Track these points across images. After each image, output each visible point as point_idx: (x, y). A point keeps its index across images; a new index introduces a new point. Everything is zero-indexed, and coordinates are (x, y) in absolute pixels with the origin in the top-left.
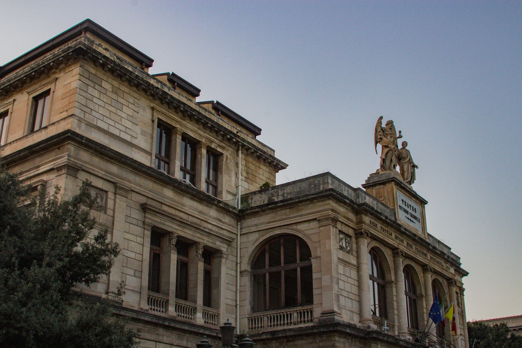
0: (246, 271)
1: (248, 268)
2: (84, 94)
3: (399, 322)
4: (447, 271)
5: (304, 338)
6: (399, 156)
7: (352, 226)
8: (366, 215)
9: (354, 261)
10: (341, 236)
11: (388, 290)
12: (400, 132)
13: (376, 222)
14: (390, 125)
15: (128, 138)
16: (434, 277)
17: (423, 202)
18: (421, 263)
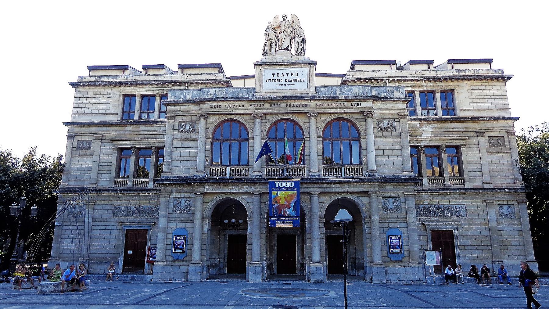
2: (78, 102)
8: (205, 104)
15: (104, 112)
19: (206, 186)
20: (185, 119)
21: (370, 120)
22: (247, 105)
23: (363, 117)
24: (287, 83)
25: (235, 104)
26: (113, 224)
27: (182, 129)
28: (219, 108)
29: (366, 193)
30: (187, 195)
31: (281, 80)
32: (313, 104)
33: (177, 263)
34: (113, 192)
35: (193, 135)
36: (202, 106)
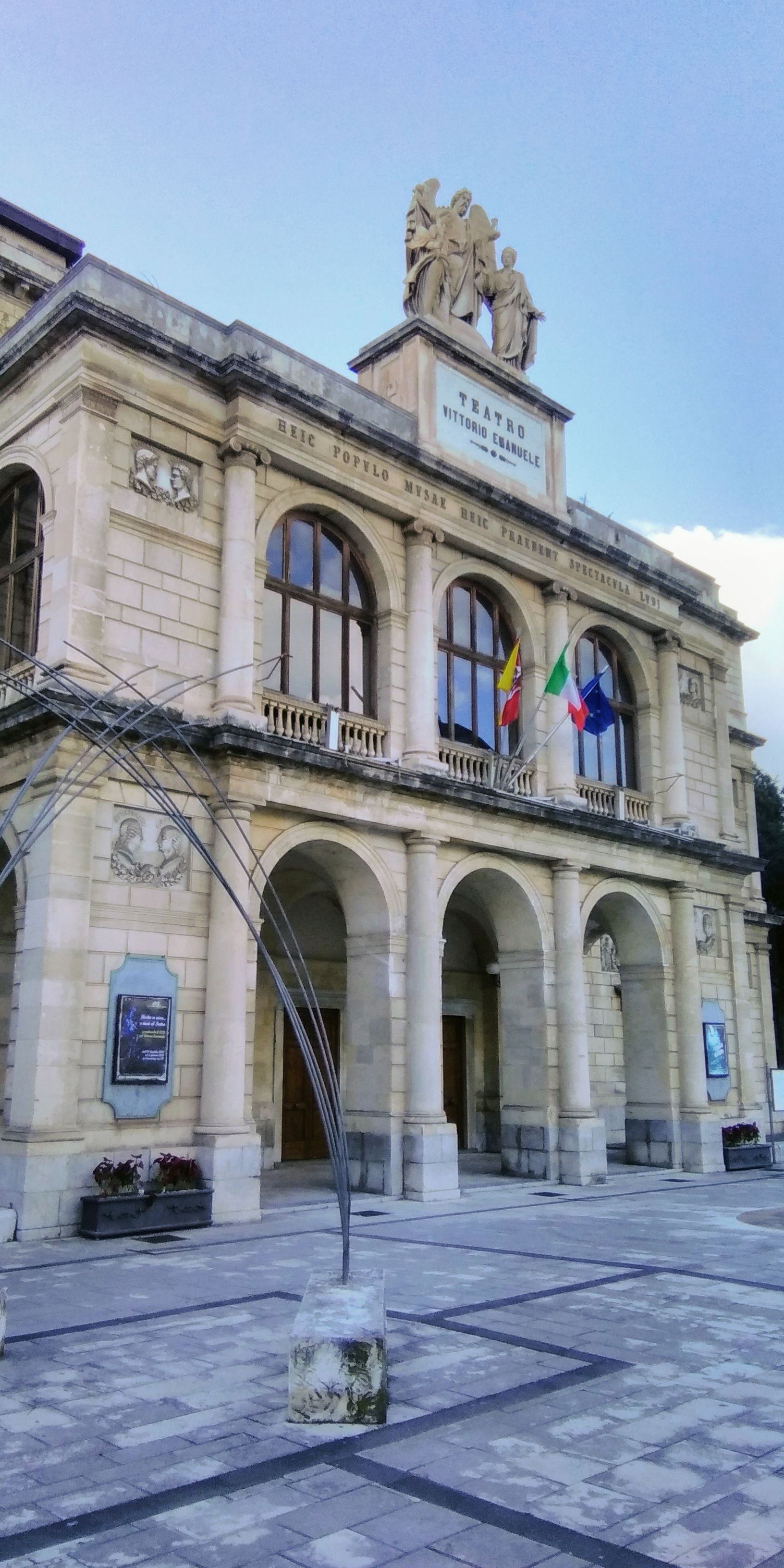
3: (407, 724)
4: (643, 607)
7: (202, 431)
9: (209, 537)
10: (146, 453)
13: (309, 430)
14: (461, 202)
16: (593, 619)
17: (556, 414)
18: (538, 579)
19: (274, 775)
20: (160, 433)
21: (672, 658)
22: (397, 477)
23: (653, 647)
24: (500, 451)
25: (361, 456)
27: (142, 476)
28: (306, 445)
29: (668, 886)
31: (483, 432)
32: (564, 557)
35: (196, 527)
36: (244, 405)
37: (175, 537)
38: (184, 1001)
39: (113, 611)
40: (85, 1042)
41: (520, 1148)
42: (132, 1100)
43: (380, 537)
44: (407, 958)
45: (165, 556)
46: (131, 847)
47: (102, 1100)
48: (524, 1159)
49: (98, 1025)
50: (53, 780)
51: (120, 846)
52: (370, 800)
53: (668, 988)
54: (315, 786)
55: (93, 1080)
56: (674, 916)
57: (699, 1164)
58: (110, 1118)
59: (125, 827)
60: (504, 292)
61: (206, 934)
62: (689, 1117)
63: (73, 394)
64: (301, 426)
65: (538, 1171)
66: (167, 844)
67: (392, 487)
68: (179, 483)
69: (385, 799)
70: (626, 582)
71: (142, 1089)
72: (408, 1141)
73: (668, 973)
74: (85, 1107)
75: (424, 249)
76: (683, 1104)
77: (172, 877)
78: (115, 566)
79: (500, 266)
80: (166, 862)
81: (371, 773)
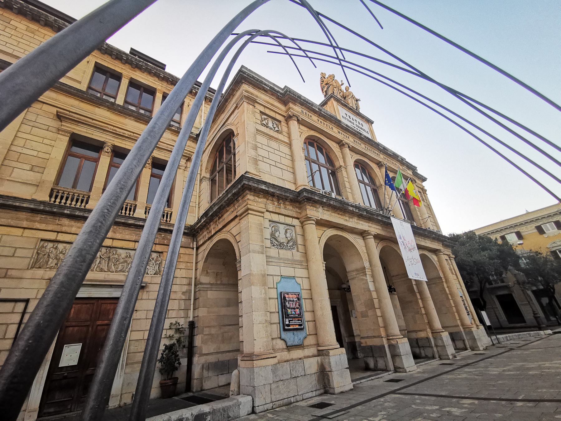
0: (204, 177)
1: (208, 176)
5: (228, 209)
6: (343, 95)
9: (286, 140)
11: (339, 175)
12: (342, 81)
13: (310, 114)
20: (267, 112)
22: (335, 130)
26: (25, 283)
27: (264, 122)
30: (289, 220)
33: (297, 354)
34: (36, 210)
37: (276, 139)
38: (304, 294)
39: (261, 158)
40: (270, 313)
41: (419, 347)
42: (292, 338)
43: (334, 146)
44: (373, 276)
45: (274, 144)
46: (277, 235)
47: (280, 338)
48: (422, 352)
49: (274, 305)
50: (248, 209)
51: (273, 235)
52: (351, 220)
53: (445, 284)
54: (333, 214)
55: (275, 330)
56: (439, 260)
57: (478, 347)
58: (285, 347)
59: (273, 228)
60: (348, 96)
61: (307, 268)
62: (467, 329)
63: (242, 99)
64: (308, 113)
65: (430, 355)
66: (288, 235)
67: (335, 132)
68: (275, 126)
69: (355, 220)
70: (398, 164)
71: (295, 332)
72: (393, 347)
73: (444, 280)
74: (274, 341)
75: (327, 84)
76: (463, 325)
77: (292, 248)
78: (260, 145)
79: (345, 91)
80: (289, 241)
81: (351, 208)
